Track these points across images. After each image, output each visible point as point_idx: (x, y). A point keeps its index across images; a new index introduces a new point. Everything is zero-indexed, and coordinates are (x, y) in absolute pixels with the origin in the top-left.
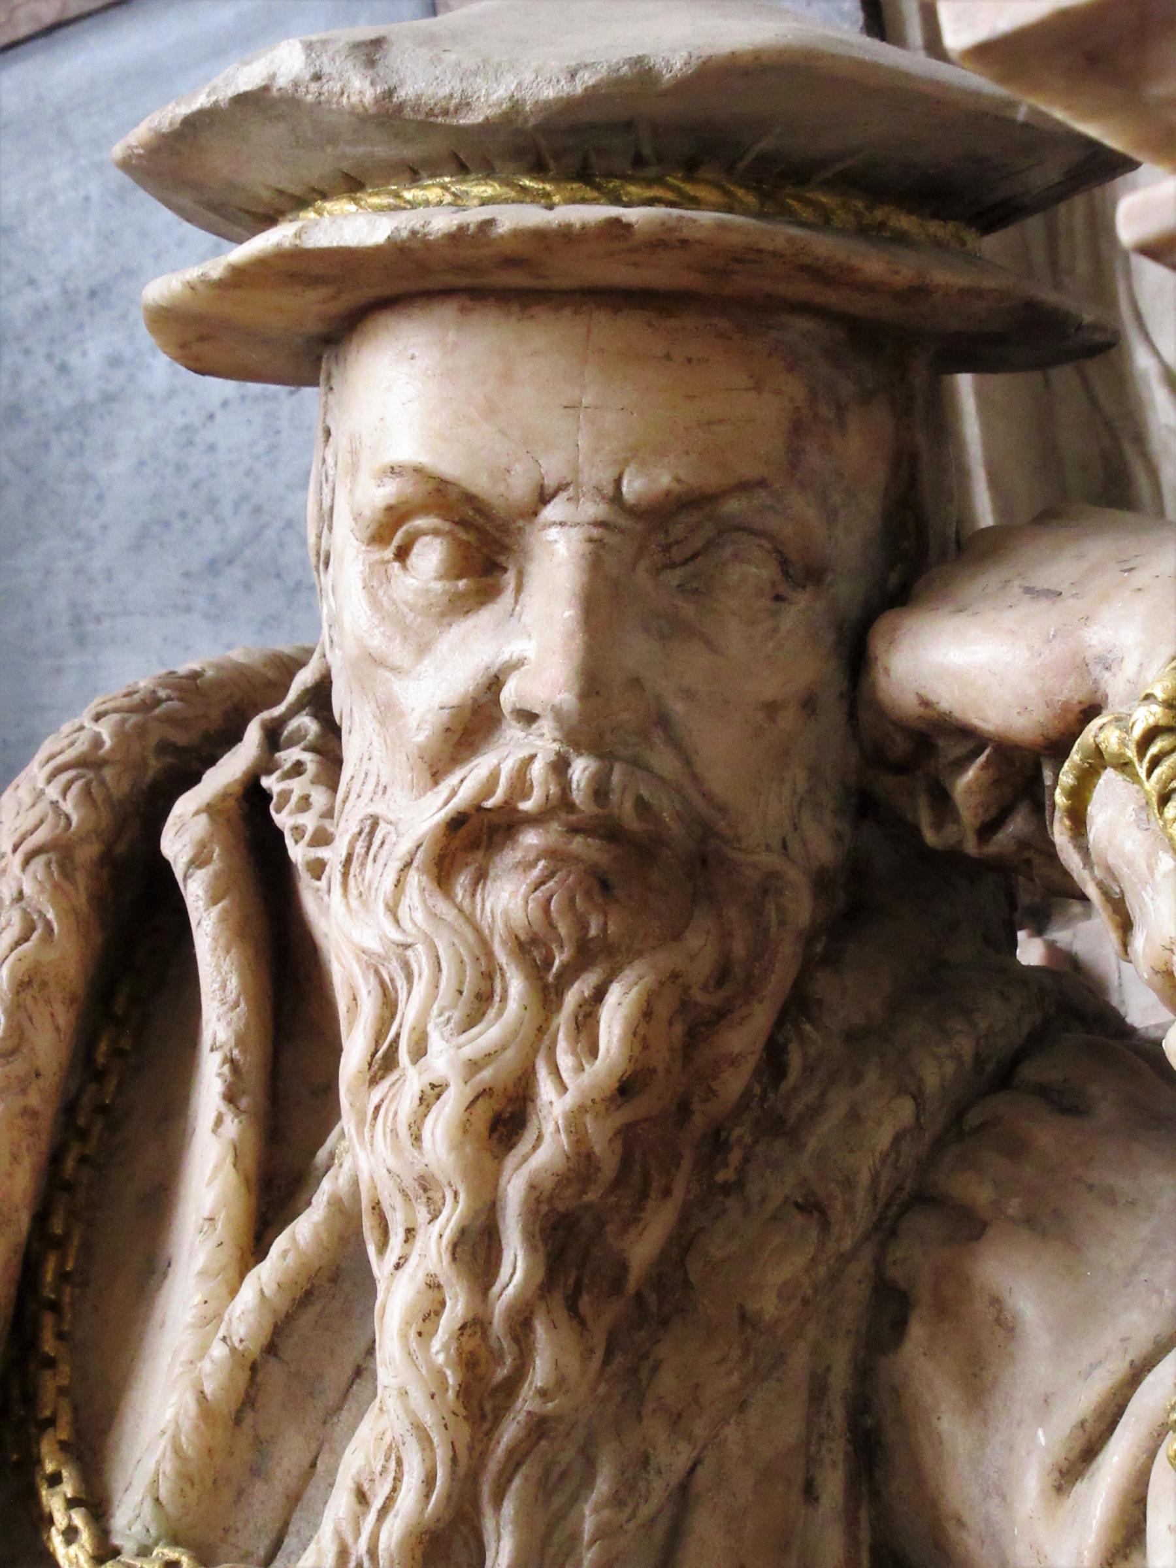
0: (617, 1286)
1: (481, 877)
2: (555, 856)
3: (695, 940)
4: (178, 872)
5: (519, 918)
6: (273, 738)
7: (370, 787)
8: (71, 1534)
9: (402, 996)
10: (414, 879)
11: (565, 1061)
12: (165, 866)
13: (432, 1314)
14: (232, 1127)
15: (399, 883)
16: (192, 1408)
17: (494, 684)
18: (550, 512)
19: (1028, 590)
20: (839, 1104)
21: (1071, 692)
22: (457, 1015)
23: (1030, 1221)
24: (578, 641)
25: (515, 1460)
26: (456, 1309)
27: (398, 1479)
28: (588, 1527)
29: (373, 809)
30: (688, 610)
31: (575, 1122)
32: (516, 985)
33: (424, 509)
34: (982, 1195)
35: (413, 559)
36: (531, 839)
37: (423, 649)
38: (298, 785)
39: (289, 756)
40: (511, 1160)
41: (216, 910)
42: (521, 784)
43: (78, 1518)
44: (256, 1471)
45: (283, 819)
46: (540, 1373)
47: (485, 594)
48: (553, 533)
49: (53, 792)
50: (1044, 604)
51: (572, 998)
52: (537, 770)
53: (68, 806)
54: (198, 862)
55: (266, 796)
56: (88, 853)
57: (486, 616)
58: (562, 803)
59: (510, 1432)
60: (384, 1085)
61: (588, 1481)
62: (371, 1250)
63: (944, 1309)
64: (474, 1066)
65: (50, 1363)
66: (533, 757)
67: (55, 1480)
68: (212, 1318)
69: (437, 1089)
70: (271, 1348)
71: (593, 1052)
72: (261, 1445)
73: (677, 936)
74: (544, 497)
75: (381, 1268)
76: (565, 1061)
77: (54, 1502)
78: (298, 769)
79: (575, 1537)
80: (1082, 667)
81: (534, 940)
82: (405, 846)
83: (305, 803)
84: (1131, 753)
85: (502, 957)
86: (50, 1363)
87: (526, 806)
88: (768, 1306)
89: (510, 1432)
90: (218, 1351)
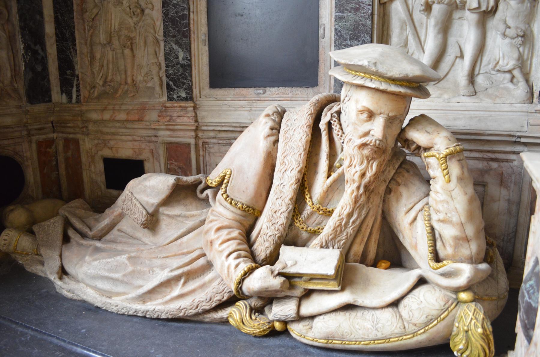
0: (369, 191)
1: (363, 149)
2: (372, 149)
3: (383, 158)
4: (322, 131)
5: (367, 155)
6: (332, 116)
7: (351, 135)
8: (309, 201)
9: (353, 159)
10: (356, 148)
11: (370, 171)
12: (320, 130)
13: (352, 193)
14: (327, 162)
15: (354, 148)
16: (322, 191)
17: (370, 131)
18: (381, 115)
19: (426, 131)
20: (388, 169)
21: (430, 145)
22: (360, 164)
23: (404, 185)
24: (382, 132)
25: (358, 208)
26: (355, 194)
27: (346, 208)
28: (363, 213)
29: (352, 138)
30: (390, 124)
31: (370, 177)
32: (365, 162)
33: (366, 111)
34: (400, 181)
35: (362, 115)
36: (369, 147)
37: (362, 125)
38: (336, 123)
39: (334, 119)
40: (363, 180)
41: (326, 136)
42: (371, 142)
43: (310, 200)
44: (327, 197)
45: (333, 127)
46: (362, 199)
47: (370, 120)
48: (380, 118)
49: (308, 118)
50: (428, 134)
51: (371, 163)
52: (373, 141)
53: (310, 120)
54: (324, 130)
55: (331, 123)
56: (312, 126)
57: (370, 123)
58: (375, 145)
59: (358, 205)
60: (349, 168)
61: (363, 209)
62: (346, 184)
63: (395, 192)
64: (361, 170)
65: (305, 181)
66: (372, 140)
67: (307, 195)
68: (324, 182)
69: (357, 172)
70: (330, 186)
71: (372, 169)
72: (328, 195)
73: (381, 157)
74: (381, 114)
75: (347, 186)
76: (370, 171)
77: (308, 197)
78: (335, 121)
79: (362, 214)
80: (433, 144)
81: (368, 157)
82: (356, 144)
83: (336, 126)
84: (439, 158)
85: (365, 158)
86: (305, 181)
87: (371, 144)
88: (381, 192)
89: (358, 205)
90: (325, 186)
